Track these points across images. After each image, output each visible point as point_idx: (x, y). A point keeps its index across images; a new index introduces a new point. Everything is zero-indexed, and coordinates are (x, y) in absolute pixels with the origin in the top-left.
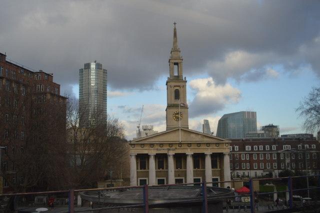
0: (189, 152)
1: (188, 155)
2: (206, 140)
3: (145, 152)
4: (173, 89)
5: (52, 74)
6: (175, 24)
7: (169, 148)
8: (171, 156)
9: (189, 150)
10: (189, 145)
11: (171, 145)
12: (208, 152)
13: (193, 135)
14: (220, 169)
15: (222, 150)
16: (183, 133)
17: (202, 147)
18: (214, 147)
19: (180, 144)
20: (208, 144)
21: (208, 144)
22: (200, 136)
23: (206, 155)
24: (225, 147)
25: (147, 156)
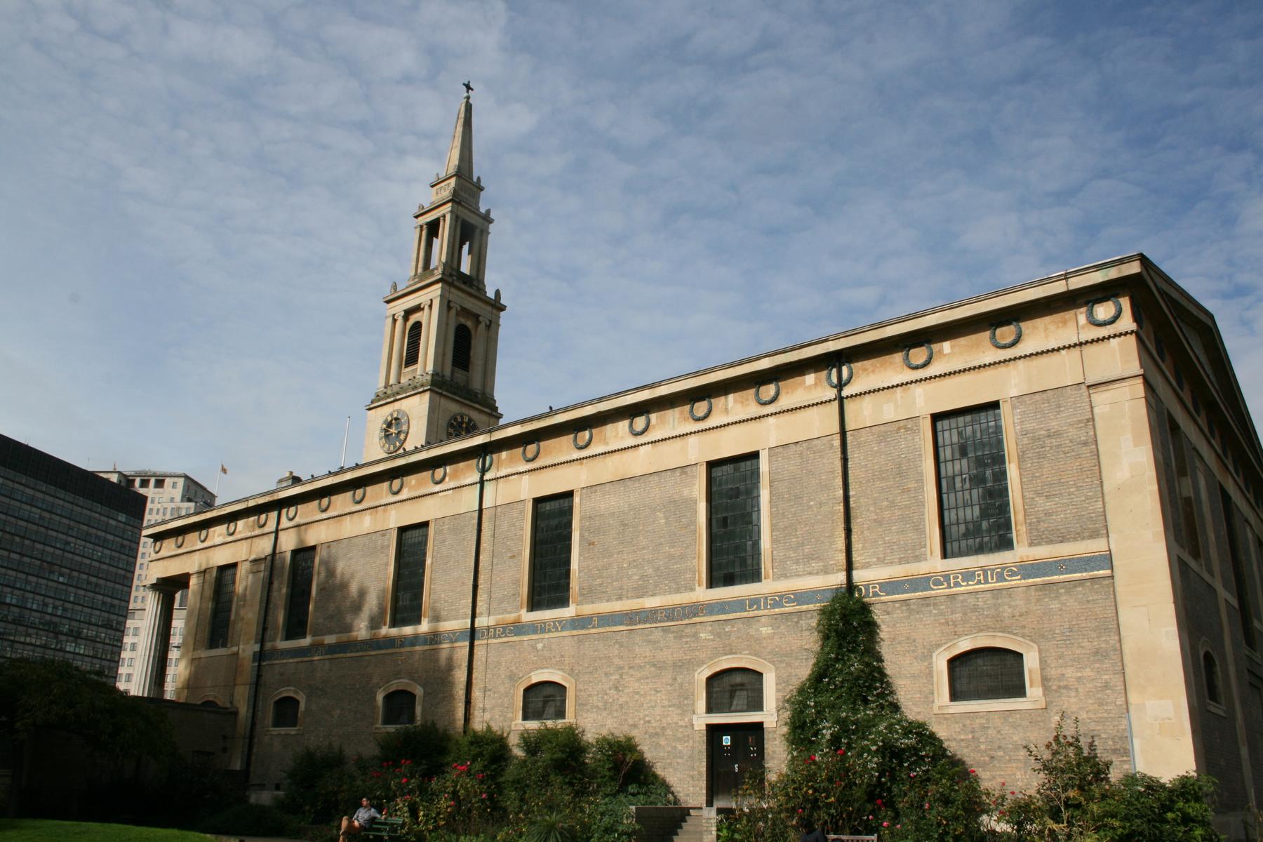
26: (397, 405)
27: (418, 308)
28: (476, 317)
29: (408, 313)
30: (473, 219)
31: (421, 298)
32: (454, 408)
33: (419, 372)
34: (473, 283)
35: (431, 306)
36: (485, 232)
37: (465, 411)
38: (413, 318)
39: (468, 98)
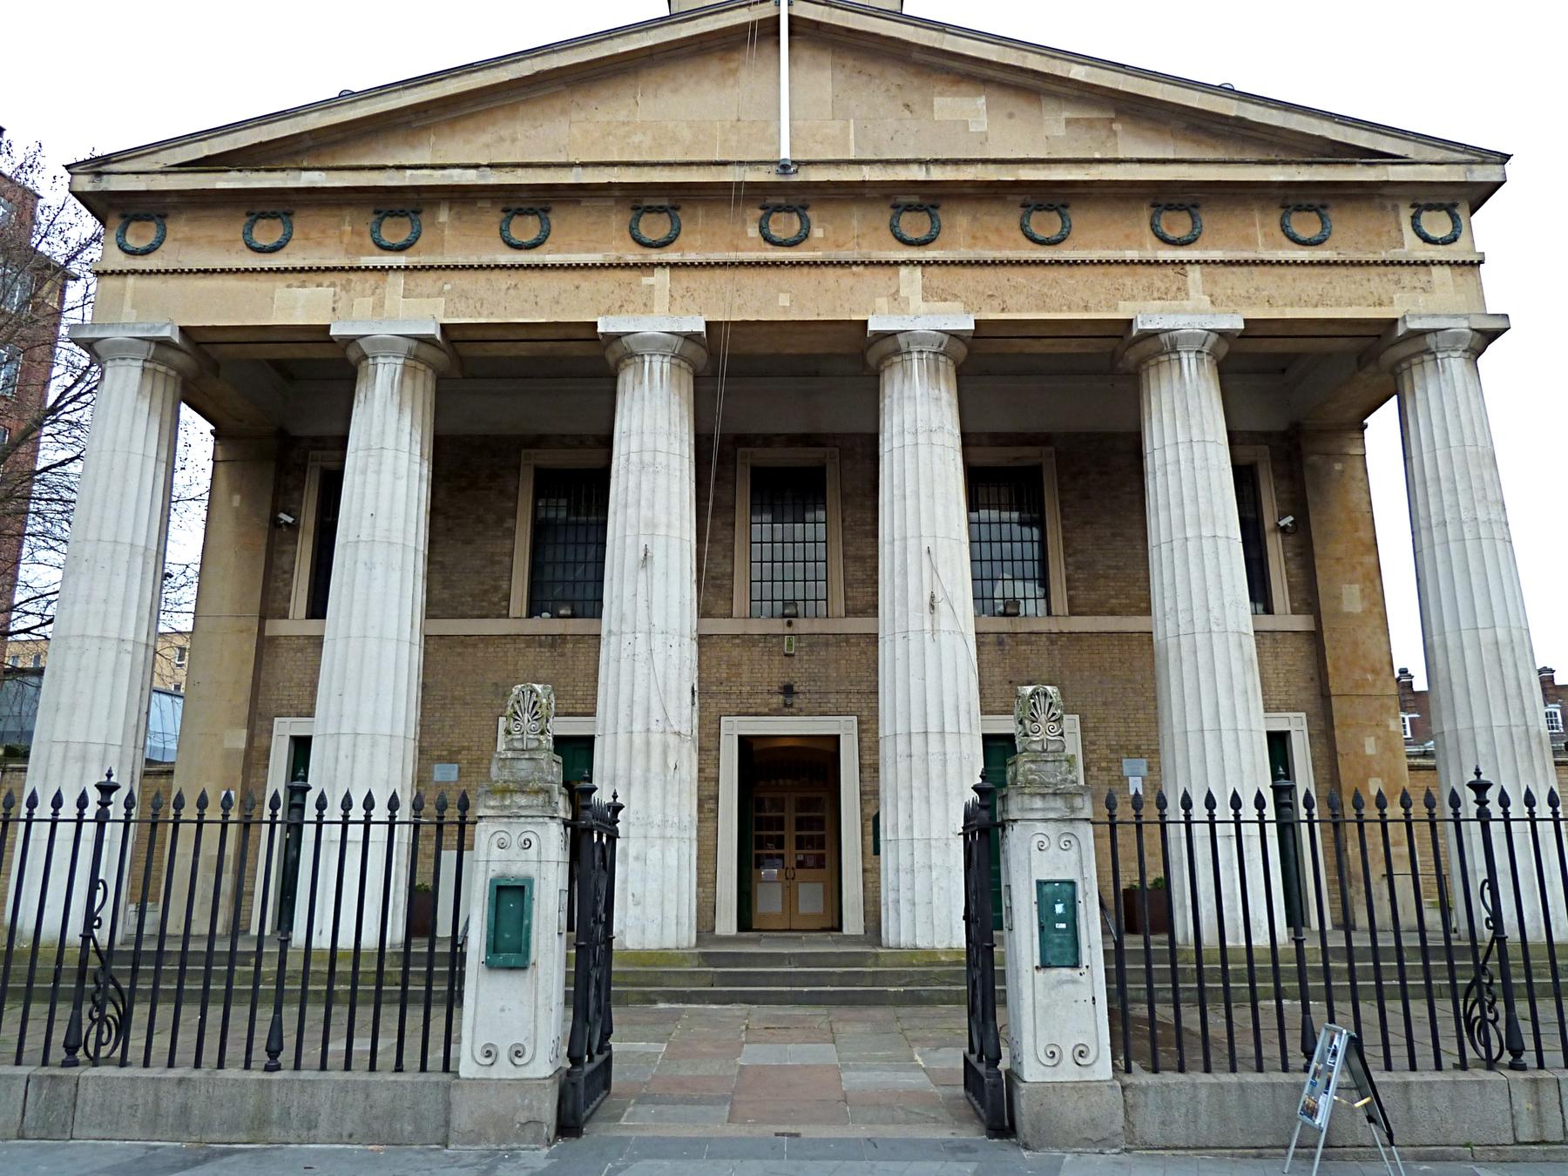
0: (917, 306)
2: (1139, 157)
3: (294, 305)
7: (634, 255)
8: (658, 367)
11: (658, 205)
12: (1189, 301)
14: (1301, 623)
15: (1376, 281)
17: (1095, 238)
18: (1260, 237)
19: (787, 198)
23: (1156, 348)
24: (1413, 248)
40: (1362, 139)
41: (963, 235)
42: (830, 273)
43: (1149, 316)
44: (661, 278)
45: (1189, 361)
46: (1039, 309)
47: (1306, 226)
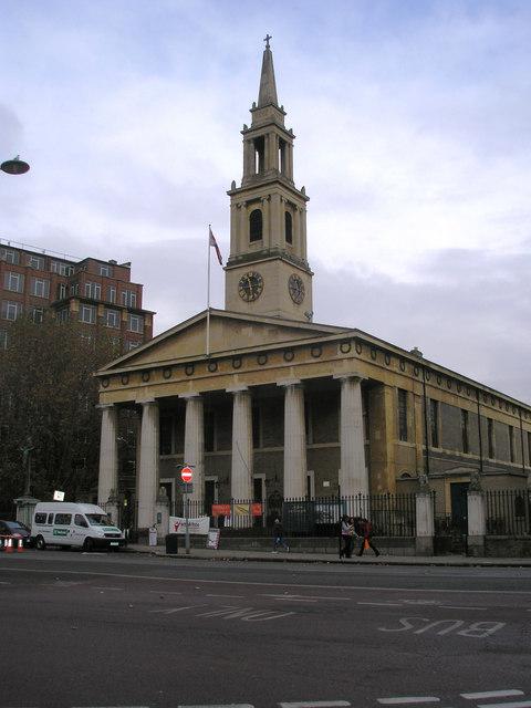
1: (231, 396)
3: (130, 396)
4: (245, 214)
5: (129, 264)
6: (268, 39)
7: (185, 377)
9: (236, 377)
10: (237, 359)
11: (190, 366)
13: (247, 331)
15: (330, 366)
16: (219, 328)
19: (212, 362)
20: (288, 352)
21: (288, 352)
22: (265, 332)
25: (139, 408)
26: (251, 269)
27: (257, 200)
28: (293, 206)
29: (249, 203)
30: (285, 138)
31: (262, 193)
32: (292, 271)
33: (266, 245)
34: (285, 180)
35: (269, 200)
36: (291, 145)
37: (296, 271)
38: (255, 207)
39: (268, 47)
40: (324, 330)
41: (247, 366)
42: (221, 378)
43: (281, 382)
44: (191, 383)
45: (289, 391)
46: (261, 381)
47: (317, 352)
